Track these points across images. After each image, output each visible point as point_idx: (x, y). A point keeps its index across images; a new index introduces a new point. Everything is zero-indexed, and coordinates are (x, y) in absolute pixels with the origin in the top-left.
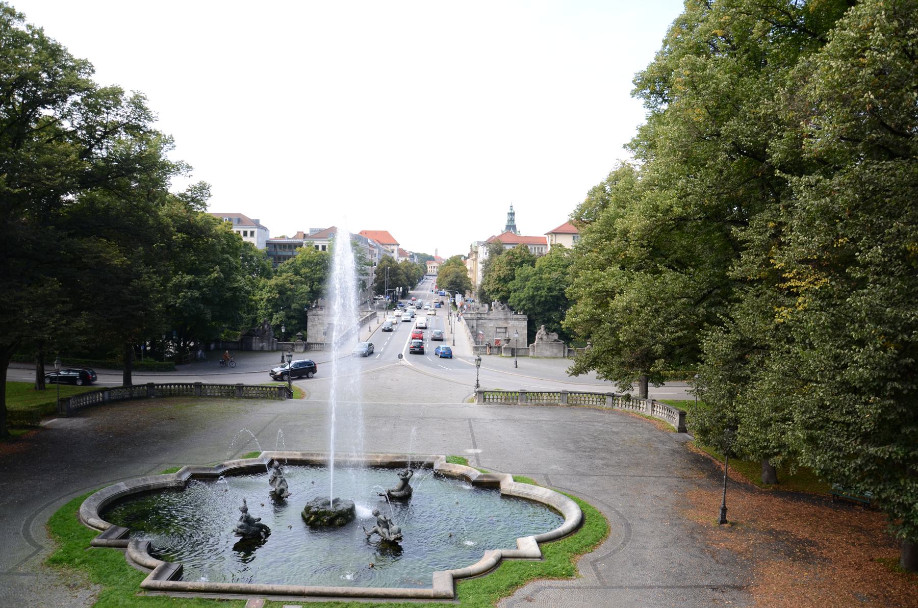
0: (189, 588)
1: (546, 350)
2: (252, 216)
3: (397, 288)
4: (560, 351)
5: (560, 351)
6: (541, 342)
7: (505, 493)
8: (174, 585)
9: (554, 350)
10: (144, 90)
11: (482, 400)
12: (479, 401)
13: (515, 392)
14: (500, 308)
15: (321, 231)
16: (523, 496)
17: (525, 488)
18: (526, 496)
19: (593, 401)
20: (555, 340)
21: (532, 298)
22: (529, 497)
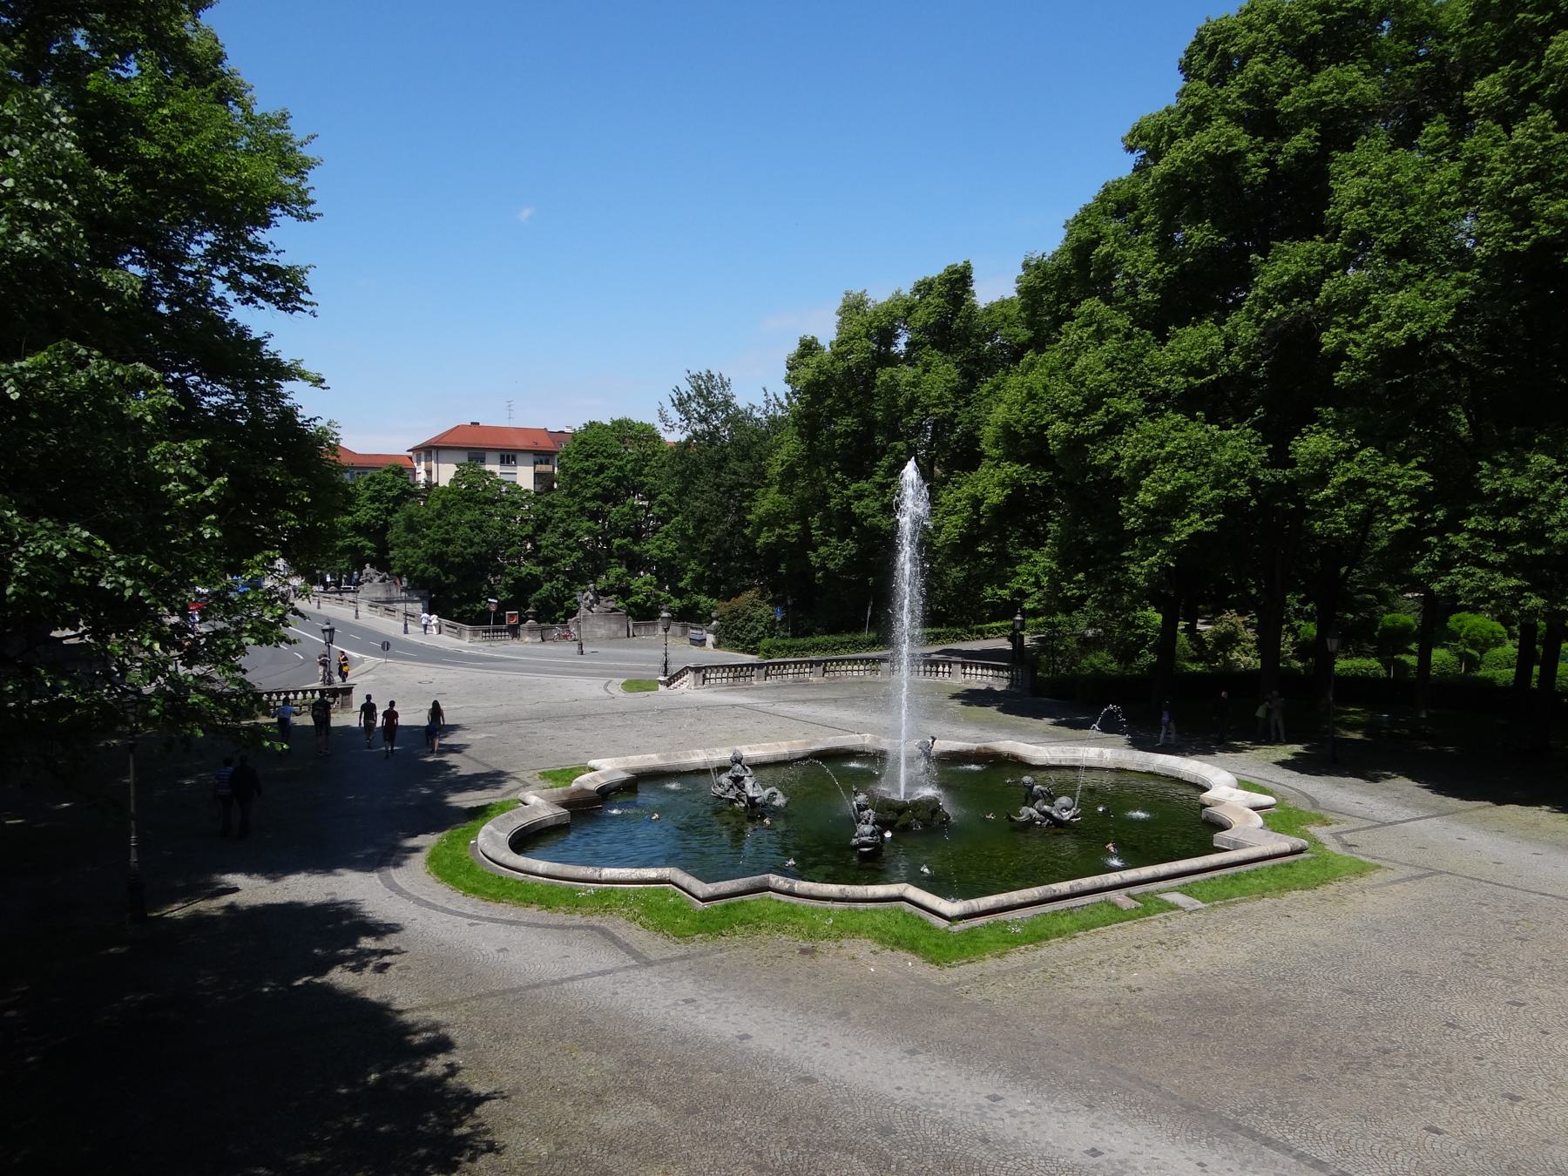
4: (622, 626)
7: (1039, 763)
12: (695, 684)
14: (376, 580)
16: (1068, 763)
18: (1072, 764)
21: (437, 559)
22: (1077, 764)
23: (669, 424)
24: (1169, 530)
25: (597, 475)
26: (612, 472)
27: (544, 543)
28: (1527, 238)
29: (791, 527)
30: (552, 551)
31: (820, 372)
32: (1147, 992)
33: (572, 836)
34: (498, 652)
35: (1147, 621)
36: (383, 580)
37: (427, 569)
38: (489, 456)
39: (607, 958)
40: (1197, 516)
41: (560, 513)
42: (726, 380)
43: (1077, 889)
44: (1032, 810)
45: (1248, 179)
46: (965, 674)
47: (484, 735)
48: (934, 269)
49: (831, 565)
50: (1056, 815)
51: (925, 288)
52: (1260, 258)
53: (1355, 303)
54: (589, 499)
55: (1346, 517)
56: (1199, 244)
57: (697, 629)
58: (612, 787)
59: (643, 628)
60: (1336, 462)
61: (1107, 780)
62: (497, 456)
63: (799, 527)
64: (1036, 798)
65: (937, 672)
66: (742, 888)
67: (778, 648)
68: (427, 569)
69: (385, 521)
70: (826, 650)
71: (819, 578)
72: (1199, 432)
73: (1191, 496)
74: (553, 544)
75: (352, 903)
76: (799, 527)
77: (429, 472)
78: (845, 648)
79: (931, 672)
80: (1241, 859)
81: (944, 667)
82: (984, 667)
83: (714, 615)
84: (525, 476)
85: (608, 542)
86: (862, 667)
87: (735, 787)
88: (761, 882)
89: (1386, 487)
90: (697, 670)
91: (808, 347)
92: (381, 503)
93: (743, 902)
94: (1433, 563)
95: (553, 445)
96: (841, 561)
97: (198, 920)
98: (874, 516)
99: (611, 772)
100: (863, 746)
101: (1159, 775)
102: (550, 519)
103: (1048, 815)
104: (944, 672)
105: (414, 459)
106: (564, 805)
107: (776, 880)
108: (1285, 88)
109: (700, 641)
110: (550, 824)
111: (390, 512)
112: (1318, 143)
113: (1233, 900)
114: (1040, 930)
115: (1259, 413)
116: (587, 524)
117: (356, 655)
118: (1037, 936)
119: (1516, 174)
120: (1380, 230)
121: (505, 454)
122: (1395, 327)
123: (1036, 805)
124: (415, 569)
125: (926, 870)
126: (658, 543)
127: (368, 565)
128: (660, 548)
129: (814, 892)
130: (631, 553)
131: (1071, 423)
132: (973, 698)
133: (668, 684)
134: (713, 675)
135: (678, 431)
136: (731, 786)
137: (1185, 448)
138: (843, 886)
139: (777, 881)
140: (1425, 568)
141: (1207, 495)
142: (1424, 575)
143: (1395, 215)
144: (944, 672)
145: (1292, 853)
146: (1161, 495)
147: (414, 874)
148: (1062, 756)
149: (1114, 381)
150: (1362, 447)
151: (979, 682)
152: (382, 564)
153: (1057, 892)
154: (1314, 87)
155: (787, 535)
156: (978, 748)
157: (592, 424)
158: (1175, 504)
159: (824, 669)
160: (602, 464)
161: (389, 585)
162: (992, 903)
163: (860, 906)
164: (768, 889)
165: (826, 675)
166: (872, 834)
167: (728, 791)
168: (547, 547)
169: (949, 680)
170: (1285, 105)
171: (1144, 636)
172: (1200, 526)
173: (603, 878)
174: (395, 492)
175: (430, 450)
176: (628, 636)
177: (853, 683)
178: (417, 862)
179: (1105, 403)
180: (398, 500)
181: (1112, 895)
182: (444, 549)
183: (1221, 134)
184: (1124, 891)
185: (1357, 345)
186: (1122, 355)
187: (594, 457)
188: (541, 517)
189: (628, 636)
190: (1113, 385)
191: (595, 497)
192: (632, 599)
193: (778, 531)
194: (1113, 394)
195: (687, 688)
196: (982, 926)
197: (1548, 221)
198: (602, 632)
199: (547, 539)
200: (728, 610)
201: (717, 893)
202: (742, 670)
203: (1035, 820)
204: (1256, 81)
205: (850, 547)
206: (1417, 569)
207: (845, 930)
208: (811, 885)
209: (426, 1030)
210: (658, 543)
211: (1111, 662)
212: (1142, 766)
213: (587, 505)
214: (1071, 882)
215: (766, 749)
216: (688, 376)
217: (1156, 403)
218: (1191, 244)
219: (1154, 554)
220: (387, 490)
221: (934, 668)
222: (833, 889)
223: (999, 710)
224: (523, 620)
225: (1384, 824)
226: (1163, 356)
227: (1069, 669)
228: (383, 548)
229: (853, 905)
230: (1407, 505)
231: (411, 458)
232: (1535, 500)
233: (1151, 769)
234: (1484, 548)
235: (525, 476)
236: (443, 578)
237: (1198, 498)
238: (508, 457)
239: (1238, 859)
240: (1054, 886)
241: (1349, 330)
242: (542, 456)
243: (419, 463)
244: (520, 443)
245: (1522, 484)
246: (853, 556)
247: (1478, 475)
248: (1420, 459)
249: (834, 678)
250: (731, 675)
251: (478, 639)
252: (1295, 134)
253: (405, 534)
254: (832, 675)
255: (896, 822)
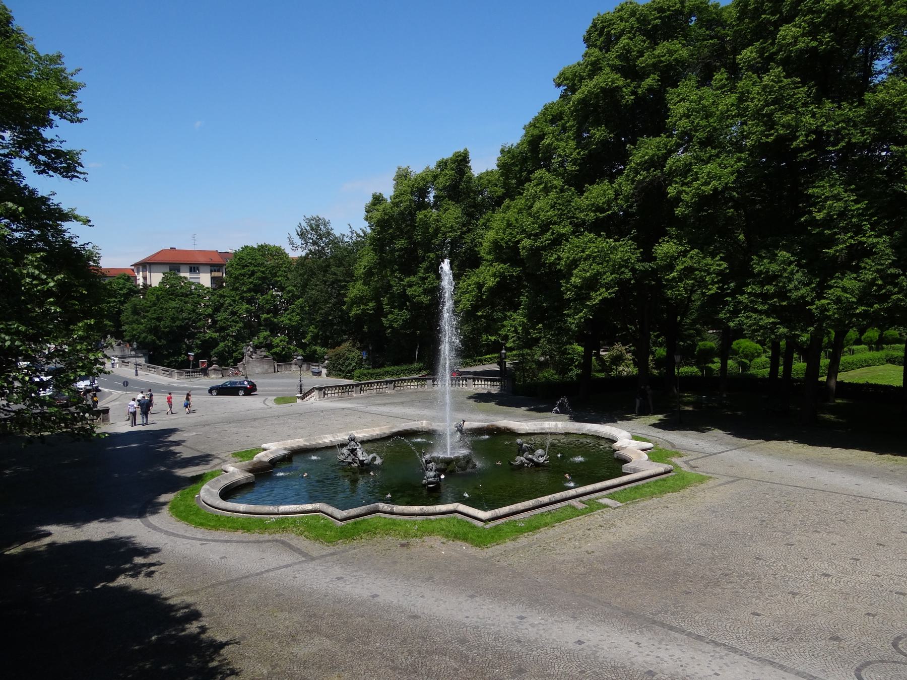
0: (522, 508)
1: (257, 367)
4: (270, 366)
5: (270, 366)
6: (251, 359)
8: (510, 509)
9: (265, 366)
12: (319, 398)
16: (538, 431)
18: (540, 431)
21: (154, 330)
22: (543, 431)
23: (295, 246)
24: (589, 299)
25: (249, 278)
26: (259, 274)
27: (219, 318)
28: (772, 135)
29: (370, 304)
30: (225, 323)
31: (385, 214)
32: (597, 554)
33: (256, 488)
34: (196, 384)
35: (574, 350)
36: (119, 345)
37: (147, 337)
38: (182, 268)
39: (288, 558)
40: (604, 290)
41: (228, 301)
42: (327, 221)
43: (553, 500)
44: (522, 458)
45: (624, 102)
46: (475, 384)
47: (194, 434)
48: (448, 155)
49: (395, 325)
50: (536, 460)
51: (443, 164)
52: (632, 147)
53: (686, 170)
54: (245, 292)
55: (684, 287)
56: (599, 138)
57: (315, 366)
58: (278, 459)
59: (283, 367)
60: (678, 256)
61: (561, 439)
62: (187, 268)
63: (374, 304)
64: (524, 451)
65: (459, 384)
66: (363, 512)
67: (365, 375)
68: (147, 337)
69: (119, 308)
70: (393, 375)
71: (389, 333)
72: (603, 243)
73: (601, 279)
74: (225, 319)
75: (129, 538)
76: (374, 304)
77: (145, 278)
78: (404, 373)
81: (463, 381)
82: (486, 380)
83: (326, 357)
84: (205, 279)
85: (258, 317)
86: (416, 383)
87: (352, 455)
88: (374, 508)
89: (705, 271)
90: (320, 389)
91: (378, 200)
92: (116, 298)
93: (364, 520)
94: (730, 312)
95: (221, 260)
96: (400, 322)
97: (28, 554)
98: (419, 296)
99: (277, 450)
100: (422, 428)
101: (589, 435)
102: (222, 305)
103: (531, 460)
104: (463, 384)
105: (135, 271)
106: (250, 471)
107: (382, 506)
108: (641, 54)
109: (318, 373)
110: (243, 483)
111: (122, 303)
112: (660, 83)
113: (637, 500)
114: (534, 523)
115: (634, 232)
116: (245, 306)
117: (106, 390)
118: (533, 528)
119: (765, 101)
120: (696, 131)
121: (193, 266)
122: (706, 183)
123: (525, 455)
124: (139, 337)
125: (467, 495)
126: (288, 316)
127: (109, 336)
128: (289, 319)
129: (405, 512)
130: (273, 323)
131: (533, 240)
132: (481, 398)
133: (303, 398)
134: (329, 392)
135: (300, 250)
136: (349, 455)
137: (596, 252)
138: (422, 507)
139: (384, 506)
140: (725, 314)
141: (609, 278)
142: (725, 318)
143: (703, 123)
144: (463, 384)
145: (665, 473)
146: (584, 279)
147: (163, 519)
148: (535, 427)
149: (555, 215)
150: (692, 249)
151: (483, 389)
152: (118, 335)
153: (542, 502)
154: (656, 53)
155: (368, 309)
156: (488, 426)
157: (246, 247)
158: (592, 284)
159: (394, 385)
160: (253, 270)
161: (123, 347)
162: (507, 511)
163: (433, 517)
164: (378, 511)
165: (396, 389)
166: (435, 477)
167: (347, 457)
168: (221, 320)
169: (466, 388)
170: (641, 62)
171: (572, 359)
172: (606, 295)
173: (280, 511)
174: (125, 291)
175: (145, 265)
176: (275, 372)
177: (411, 393)
178: (165, 510)
179: (551, 228)
180: (127, 296)
181: (572, 502)
182: (158, 324)
183: (607, 78)
184: (578, 499)
185: (687, 193)
186: (559, 201)
187: (248, 266)
188: (217, 303)
189: (275, 372)
190: (555, 218)
191: (249, 290)
192: (274, 350)
193: (362, 307)
194: (555, 223)
195: (314, 400)
196: (503, 524)
197: (783, 126)
198: (258, 370)
199: (221, 316)
200: (334, 354)
201: (349, 515)
202: (346, 388)
203: (524, 463)
204: (625, 49)
205: (406, 314)
206: (722, 315)
207: (425, 532)
208: (403, 507)
209: (183, 608)
210: (288, 316)
211: (555, 374)
212: (579, 430)
213: (245, 295)
214: (549, 496)
215: (366, 432)
216: (305, 219)
217: (579, 227)
218: (595, 138)
219: (581, 311)
220: (120, 290)
222: (416, 509)
223: (496, 404)
224: (210, 365)
225: (710, 455)
226: (582, 201)
227: (532, 379)
228: (118, 324)
229: (428, 517)
230: (716, 280)
231: (133, 270)
232: (781, 276)
233: (584, 432)
234: (756, 302)
235: (205, 279)
236: (158, 342)
237: (604, 279)
238: (194, 268)
239: (637, 478)
240: (540, 499)
241: (682, 186)
242: (214, 267)
243: (138, 273)
244: (202, 260)
245: (774, 267)
246: (407, 319)
247: (752, 263)
248: (721, 255)
249: (400, 390)
250: (340, 391)
251: (182, 377)
252: (647, 78)
253: (132, 316)
254: (399, 388)
255: (446, 469)
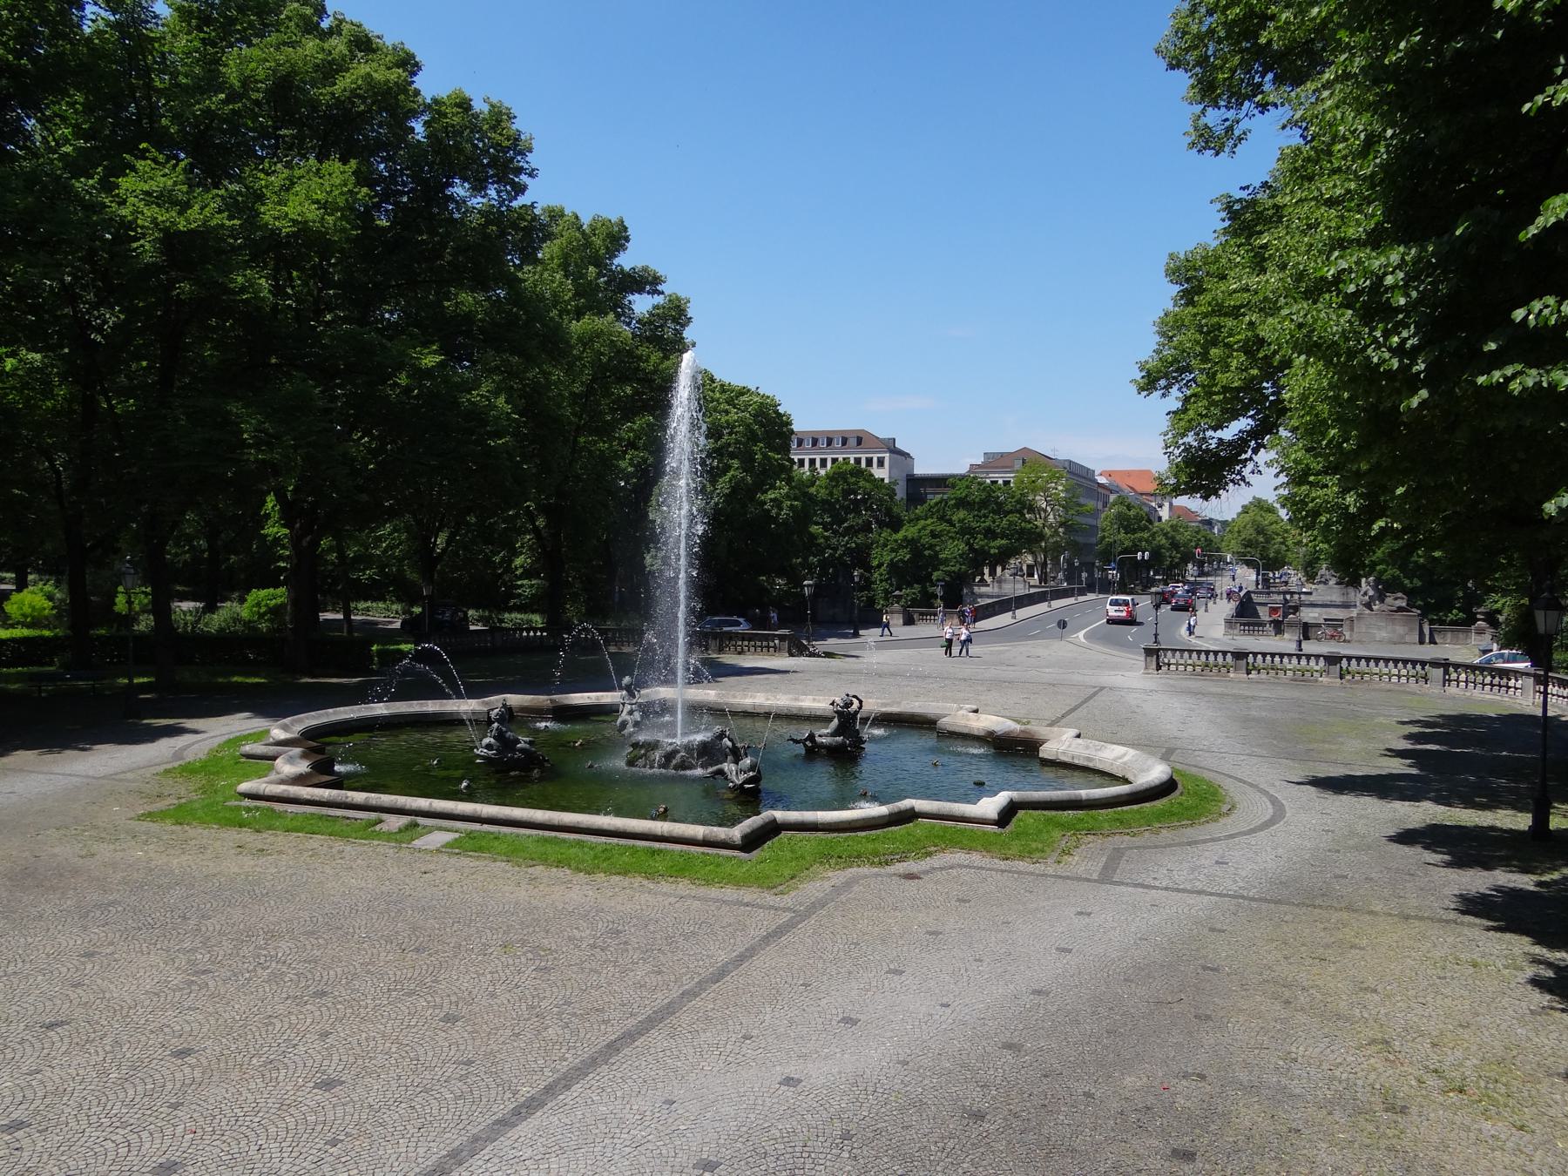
2: (882, 434)
3: (1140, 553)
4: (1411, 630)
5: (1411, 630)
6: (1368, 611)
8: (285, 790)
9: (1397, 628)
10: (508, 102)
11: (1154, 666)
13: (1225, 653)
15: (1002, 455)
17: (1087, 747)
18: (1085, 763)
19: (1399, 677)
20: (1400, 609)
22: (1091, 765)
68: (1386, 571)
79: (1500, 686)
80: (612, 828)
162: (278, 791)
176: (1422, 642)
198: (1384, 634)
221: (1504, 682)
240: (350, 793)
251: (1236, 632)
